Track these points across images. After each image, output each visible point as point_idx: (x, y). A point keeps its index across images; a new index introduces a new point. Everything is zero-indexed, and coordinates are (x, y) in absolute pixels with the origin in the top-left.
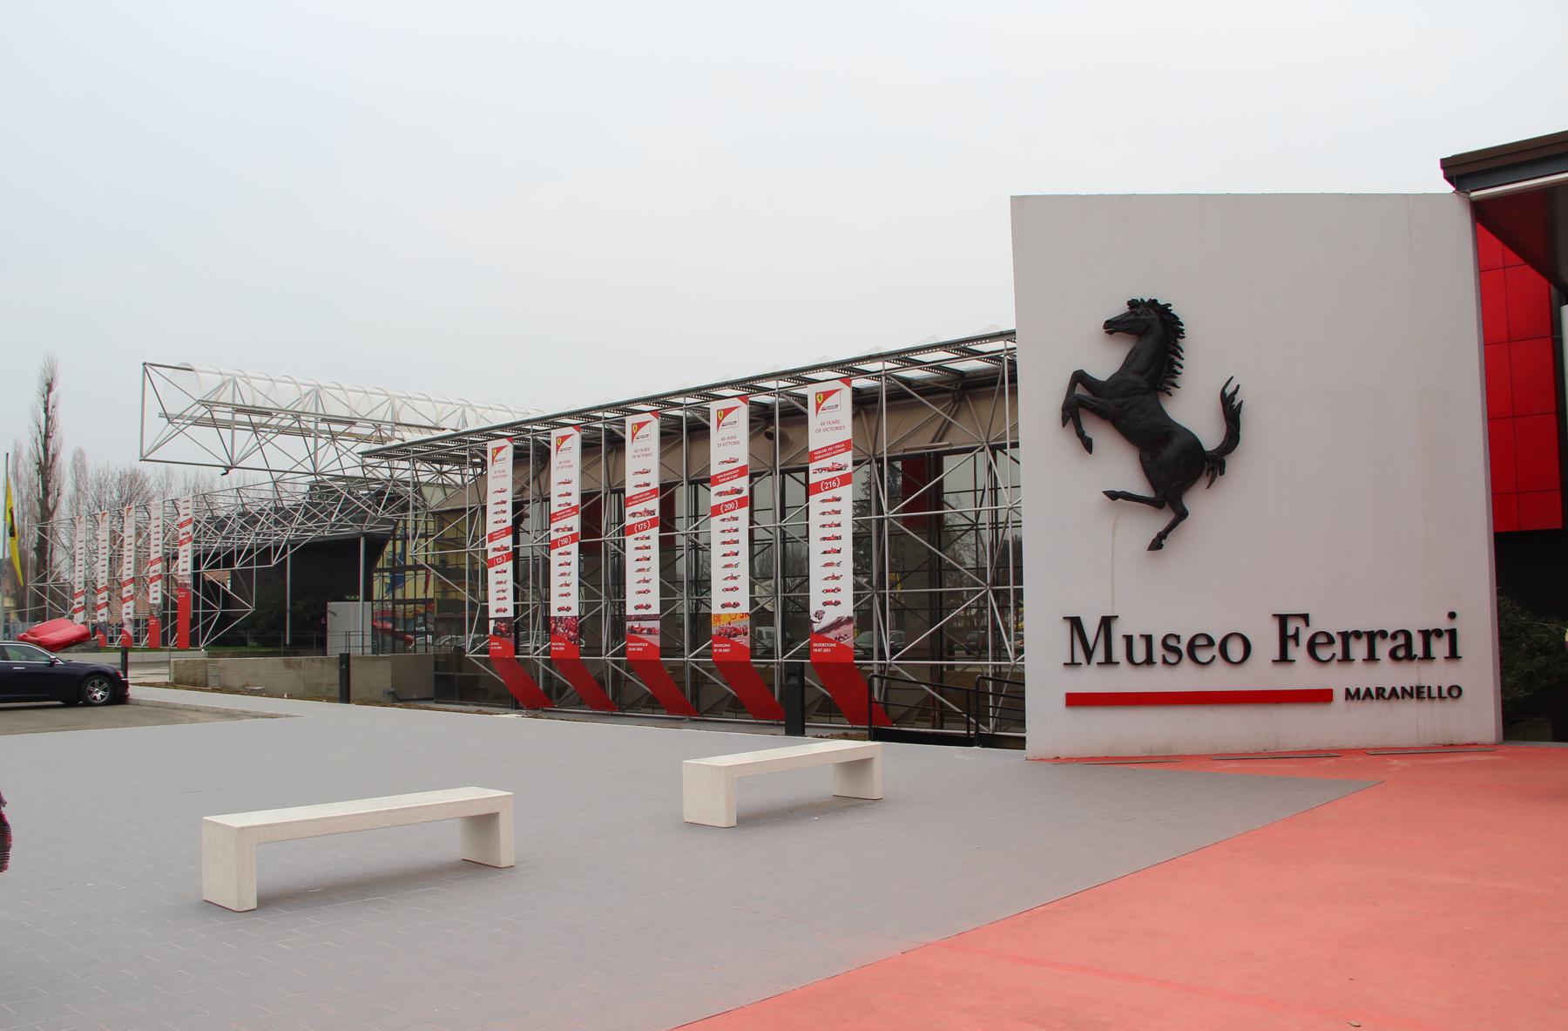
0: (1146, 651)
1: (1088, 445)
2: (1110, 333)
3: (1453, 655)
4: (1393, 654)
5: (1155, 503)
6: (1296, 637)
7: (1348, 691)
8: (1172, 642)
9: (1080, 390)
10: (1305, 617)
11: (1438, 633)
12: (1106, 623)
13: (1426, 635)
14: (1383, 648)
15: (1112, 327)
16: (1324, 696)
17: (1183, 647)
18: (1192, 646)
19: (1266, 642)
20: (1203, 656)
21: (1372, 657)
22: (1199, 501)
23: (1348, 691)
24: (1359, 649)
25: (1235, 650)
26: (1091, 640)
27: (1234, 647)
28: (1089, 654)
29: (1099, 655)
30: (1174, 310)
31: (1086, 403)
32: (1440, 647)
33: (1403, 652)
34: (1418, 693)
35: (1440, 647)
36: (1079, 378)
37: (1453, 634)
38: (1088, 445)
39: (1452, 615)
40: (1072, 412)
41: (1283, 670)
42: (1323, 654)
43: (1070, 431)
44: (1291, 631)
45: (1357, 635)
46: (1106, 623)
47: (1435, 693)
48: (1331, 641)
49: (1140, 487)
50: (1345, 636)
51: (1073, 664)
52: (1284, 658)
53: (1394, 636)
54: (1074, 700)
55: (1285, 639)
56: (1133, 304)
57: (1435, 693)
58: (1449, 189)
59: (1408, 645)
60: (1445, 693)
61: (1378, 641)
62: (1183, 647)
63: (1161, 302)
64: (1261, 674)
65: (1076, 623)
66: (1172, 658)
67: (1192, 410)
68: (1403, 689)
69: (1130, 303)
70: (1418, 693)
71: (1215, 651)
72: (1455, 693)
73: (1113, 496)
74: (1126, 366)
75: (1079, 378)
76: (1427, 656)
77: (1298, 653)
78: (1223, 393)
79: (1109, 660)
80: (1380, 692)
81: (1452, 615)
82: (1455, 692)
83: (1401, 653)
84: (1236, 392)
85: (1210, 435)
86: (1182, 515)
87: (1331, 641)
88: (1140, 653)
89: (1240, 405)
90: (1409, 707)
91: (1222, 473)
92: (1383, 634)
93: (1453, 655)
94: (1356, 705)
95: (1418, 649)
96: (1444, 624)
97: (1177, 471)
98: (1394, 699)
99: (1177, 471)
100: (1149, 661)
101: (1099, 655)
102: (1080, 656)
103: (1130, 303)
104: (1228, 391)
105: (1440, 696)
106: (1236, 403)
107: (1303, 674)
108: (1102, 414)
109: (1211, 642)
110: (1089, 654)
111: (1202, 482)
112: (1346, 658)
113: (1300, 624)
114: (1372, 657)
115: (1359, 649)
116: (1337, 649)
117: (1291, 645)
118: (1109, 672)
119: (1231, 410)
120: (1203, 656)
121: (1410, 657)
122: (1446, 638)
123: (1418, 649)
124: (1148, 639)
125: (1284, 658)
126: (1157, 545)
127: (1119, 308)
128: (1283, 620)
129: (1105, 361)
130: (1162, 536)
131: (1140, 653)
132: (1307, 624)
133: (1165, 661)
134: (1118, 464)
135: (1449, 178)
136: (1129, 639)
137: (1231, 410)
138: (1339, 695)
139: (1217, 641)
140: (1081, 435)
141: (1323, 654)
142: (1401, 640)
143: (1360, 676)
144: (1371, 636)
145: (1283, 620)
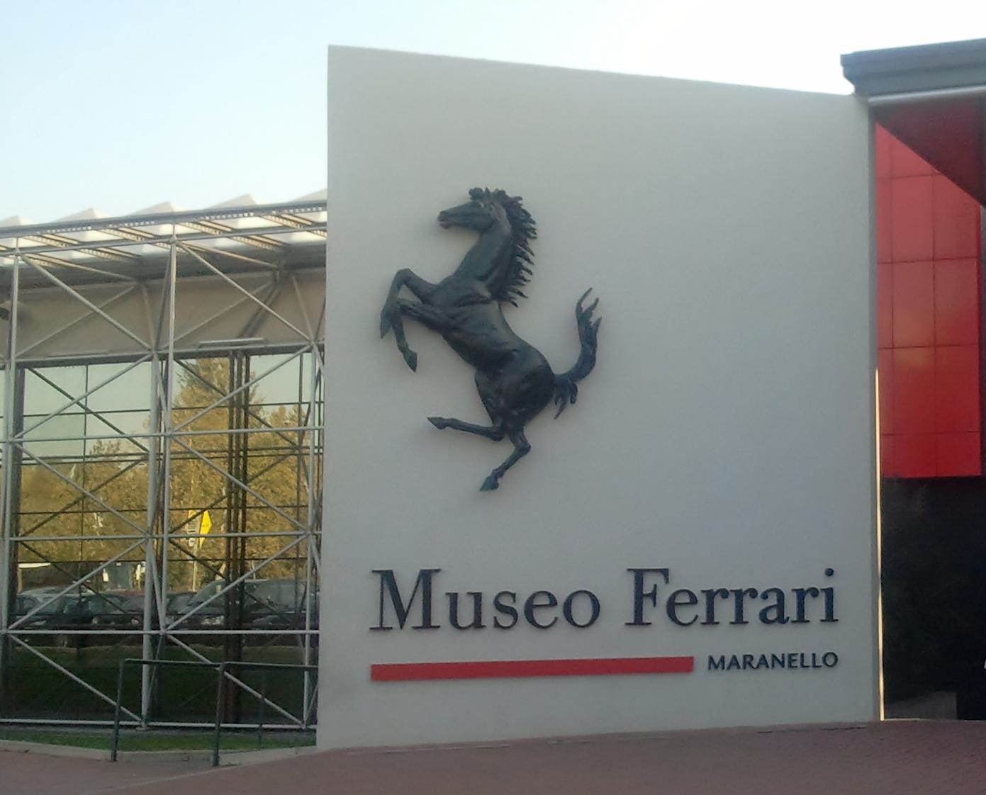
0: (477, 613)
1: (412, 362)
2: (447, 227)
3: (830, 618)
4: (763, 617)
5: (494, 435)
6: (653, 596)
7: (711, 660)
8: (506, 601)
9: (406, 295)
10: (665, 572)
11: (814, 592)
12: (426, 578)
13: (801, 594)
14: (753, 609)
15: (452, 221)
16: (683, 665)
17: (520, 607)
18: (530, 607)
19: (619, 602)
20: (543, 617)
21: (739, 620)
22: (545, 432)
23: (711, 660)
24: (725, 610)
25: (582, 611)
26: (406, 599)
27: (577, 609)
28: (402, 616)
29: (415, 617)
30: (526, 205)
31: (413, 311)
32: (815, 609)
33: (775, 615)
34: (788, 662)
35: (815, 609)
36: (405, 279)
37: (829, 593)
38: (412, 362)
39: (830, 573)
41: (638, 632)
42: (685, 615)
43: (391, 343)
44: (647, 589)
45: (724, 594)
46: (426, 578)
47: (808, 662)
48: (694, 601)
50: (710, 595)
51: (382, 628)
52: (639, 621)
53: (765, 596)
54: (383, 673)
55: (640, 597)
56: (476, 194)
57: (808, 662)
58: (848, 88)
59: (780, 605)
60: (819, 662)
61: (747, 599)
62: (520, 607)
63: (511, 194)
64: (610, 638)
65: (388, 578)
66: (506, 620)
67: (539, 323)
68: (774, 657)
69: (471, 192)
70: (788, 662)
71: (558, 612)
72: (830, 661)
73: (440, 424)
75: (405, 279)
76: (801, 619)
77: (655, 614)
78: (579, 303)
79: (427, 624)
80: (748, 660)
81: (830, 573)
82: (831, 660)
83: (772, 615)
84: (594, 306)
85: (561, 358)
86: (523, 449)
87: (694, 601)
88: (466, 615)
89: (597, 324)
90: (779, 676)
91: (573, 402)
92: (753, 593)
93: (830, 618)
94: (721, 676)
95: (791, 610)
96: (822, 583)
97: (519, 396)
98: (763, 667)
99: (519, 396)
100: (477, 624)
101: (415, 617)
102: (391, 618)
103: (471, 192)
104: (586, 305)
105: (814, 666)
106: (593, 320)
107: (661, 639)
108: (433, 325)
109: (553, 602)
110: (402, 616)
111: (551, 410)
112: (711, 620)
113: (659, 579)
114: (739, 620)
115: (725, 610)
116: (701, 610)
117: (647, 604)
118: (428, 635)
119: (587, 330)
120: (543, 617)
121: (781, 619)
122: (822, 598)
123: (791, 610)
124: (478, 597)
125: (639, 621)
126: (492, 484)
127: (457, 196)
128: (639, 575)
129: (438, 261)
130: (499, 473)
131: (466, 615)
132: (667, 581)
133: (497, 625)
134: (450, 387)
135: (849, 76)
136: (454, 598)
137: (587, 330)
138: (701, 663)
139: (561, 599)
140: (404, 349)
141: (685, 615)
142: (772, 600)
143: (725, 640)
144: (739, 595)
145: (639, 575)
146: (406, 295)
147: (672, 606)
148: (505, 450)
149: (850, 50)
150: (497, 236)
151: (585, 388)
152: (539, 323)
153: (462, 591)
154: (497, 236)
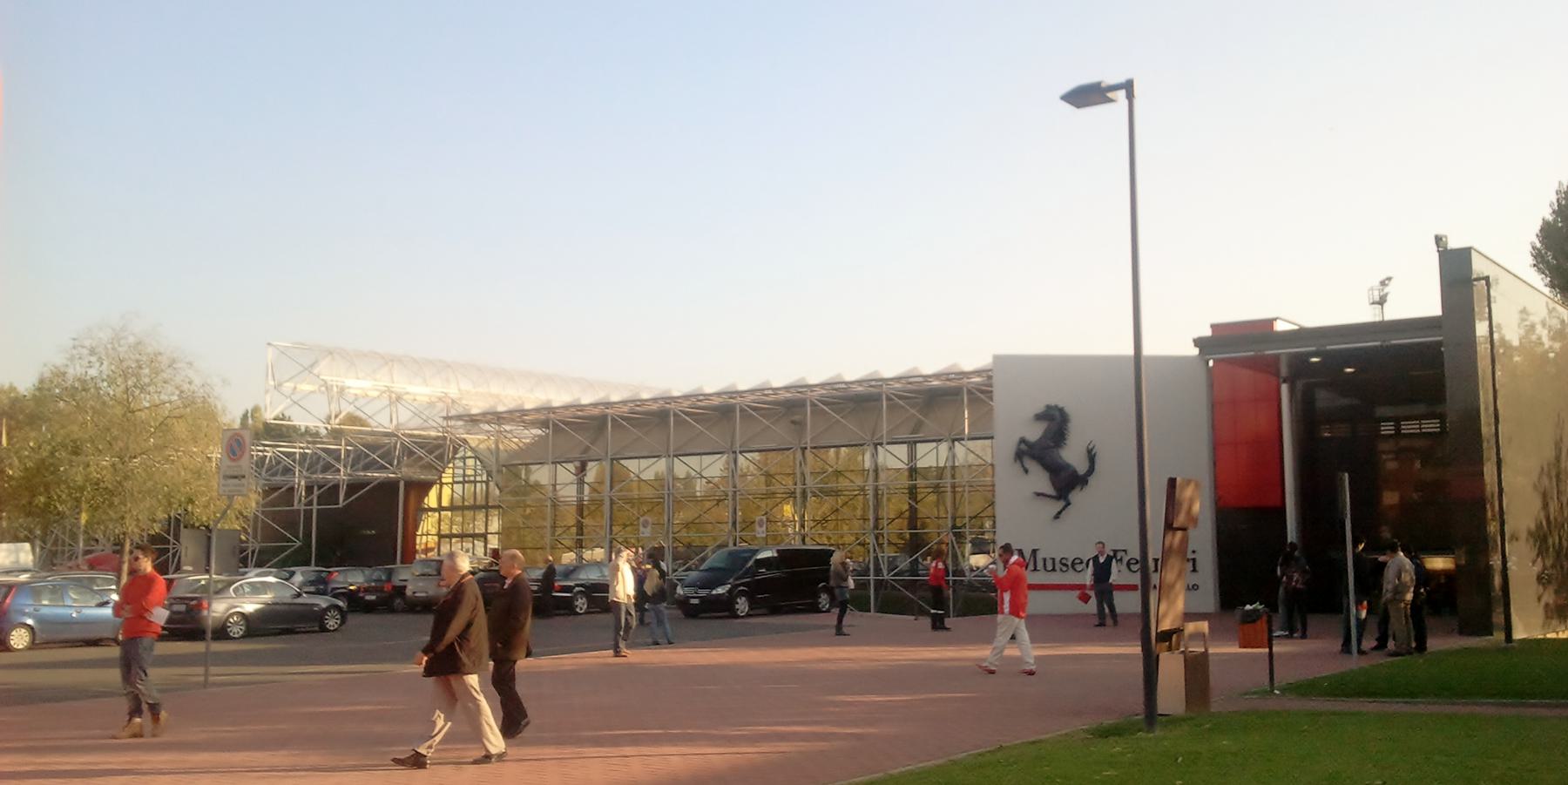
1: (1026, 471)
3: (1194, 570)
5: (1058, 498)
9: (1023, 447)
12: (1034, 551)
15: (1039, 417)
29: (1031, 567)
31: (1026, 452)
36: (1023, 441)
38: (1026, 471)
40: (1019, 456)
43: (1018, 465)
46: (1034, 551)
49: (1050, 491)
56: (1049, 407)
67: (1071, 454)
73: (1038, 494)
74: (1046, 432)
75: (1023, 441)
85: (1081, 467)
93: (1194, 570)
97: (1066, 483)
99: (1066, 483)
108: (1033, 457)
119: (1091, 457)
120: (1079, 568)
126: (1057, 517)
129: (1035, 433)
134: (1040, 480)
137: (1091, 457)
146: (1023, 447)
147: (1128, 564)
148: (1062, 504)
149: (1196, 336)
150: (1056, 422)
151: (1092, 480)
152: (1071, 454)
153: (1048, 557)
154: (1056, 422)
